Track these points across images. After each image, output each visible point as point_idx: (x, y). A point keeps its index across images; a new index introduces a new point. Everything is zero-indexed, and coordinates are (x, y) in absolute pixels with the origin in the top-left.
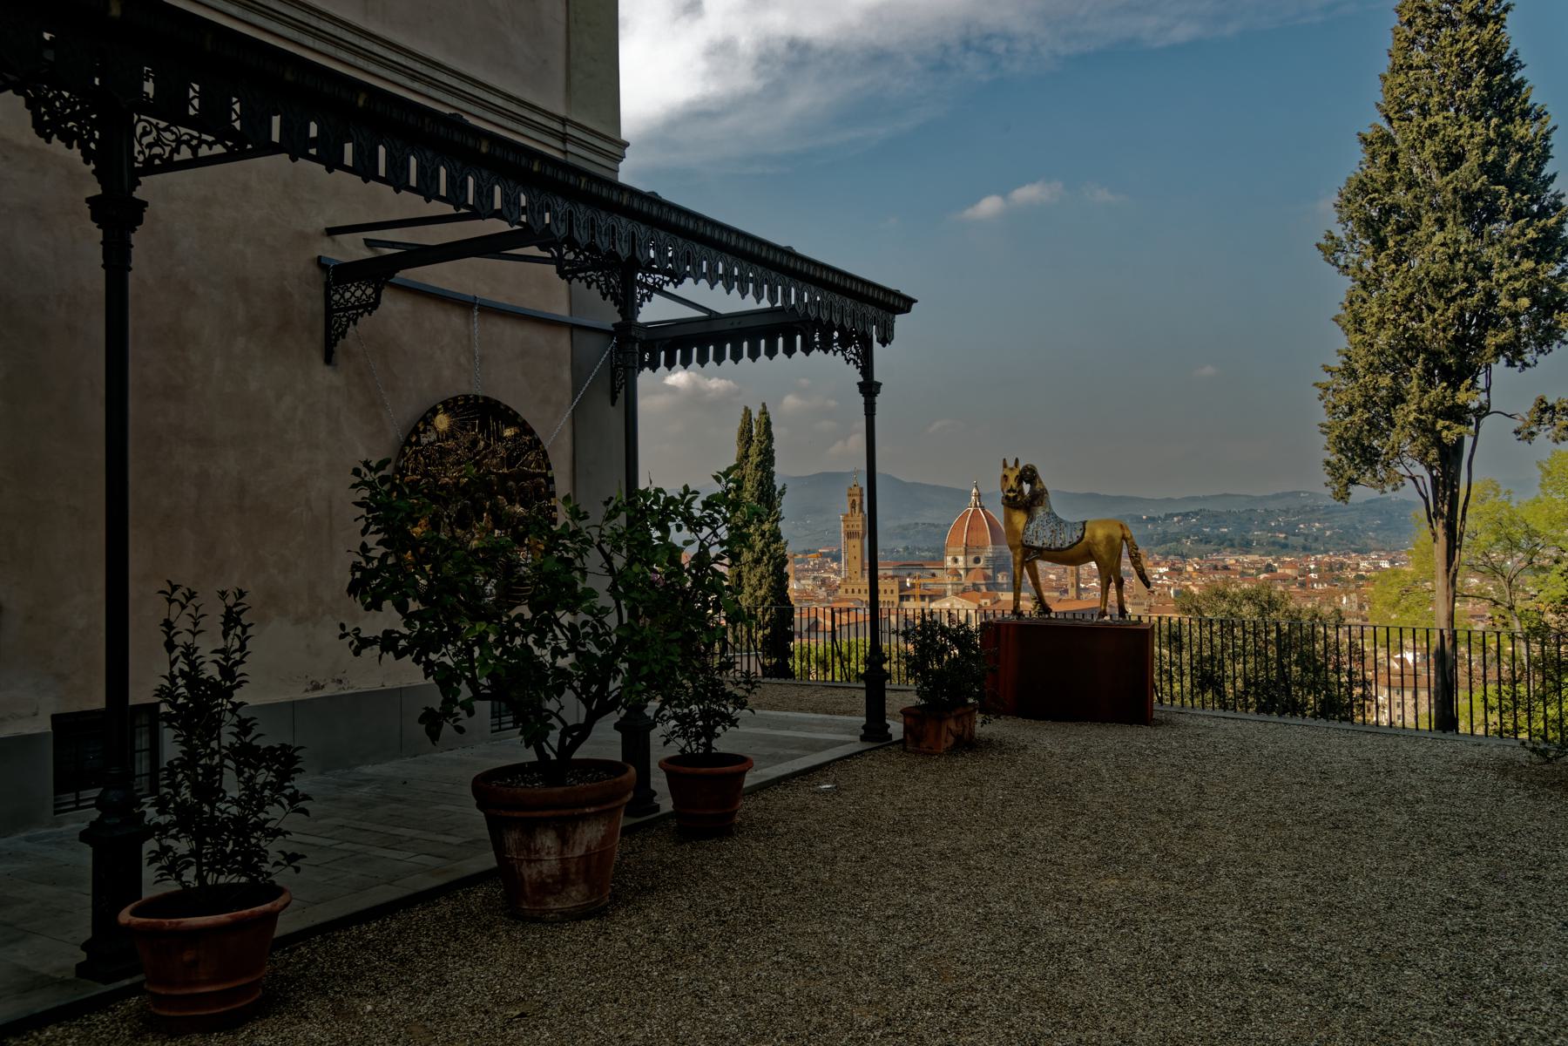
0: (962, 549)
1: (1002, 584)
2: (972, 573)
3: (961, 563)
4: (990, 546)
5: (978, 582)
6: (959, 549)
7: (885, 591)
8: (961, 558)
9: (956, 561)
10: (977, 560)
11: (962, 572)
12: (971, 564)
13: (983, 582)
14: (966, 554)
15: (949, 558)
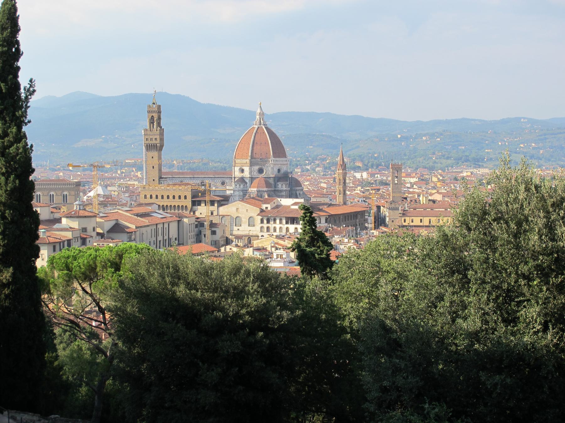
0: (248, 161)
1: (281, 191)
2: (256, 182)
3: (247, 174)
4: (272, 159)
5: (261, 189)
6: (244, 161)
7: (185, 197)
8: (247, 169)
9: (242, 171)
10: (261, 171)
11: (247, 181)
12: (255, 174)
13: (265, 189)
14: (252, 164)
15: (237, 169)
